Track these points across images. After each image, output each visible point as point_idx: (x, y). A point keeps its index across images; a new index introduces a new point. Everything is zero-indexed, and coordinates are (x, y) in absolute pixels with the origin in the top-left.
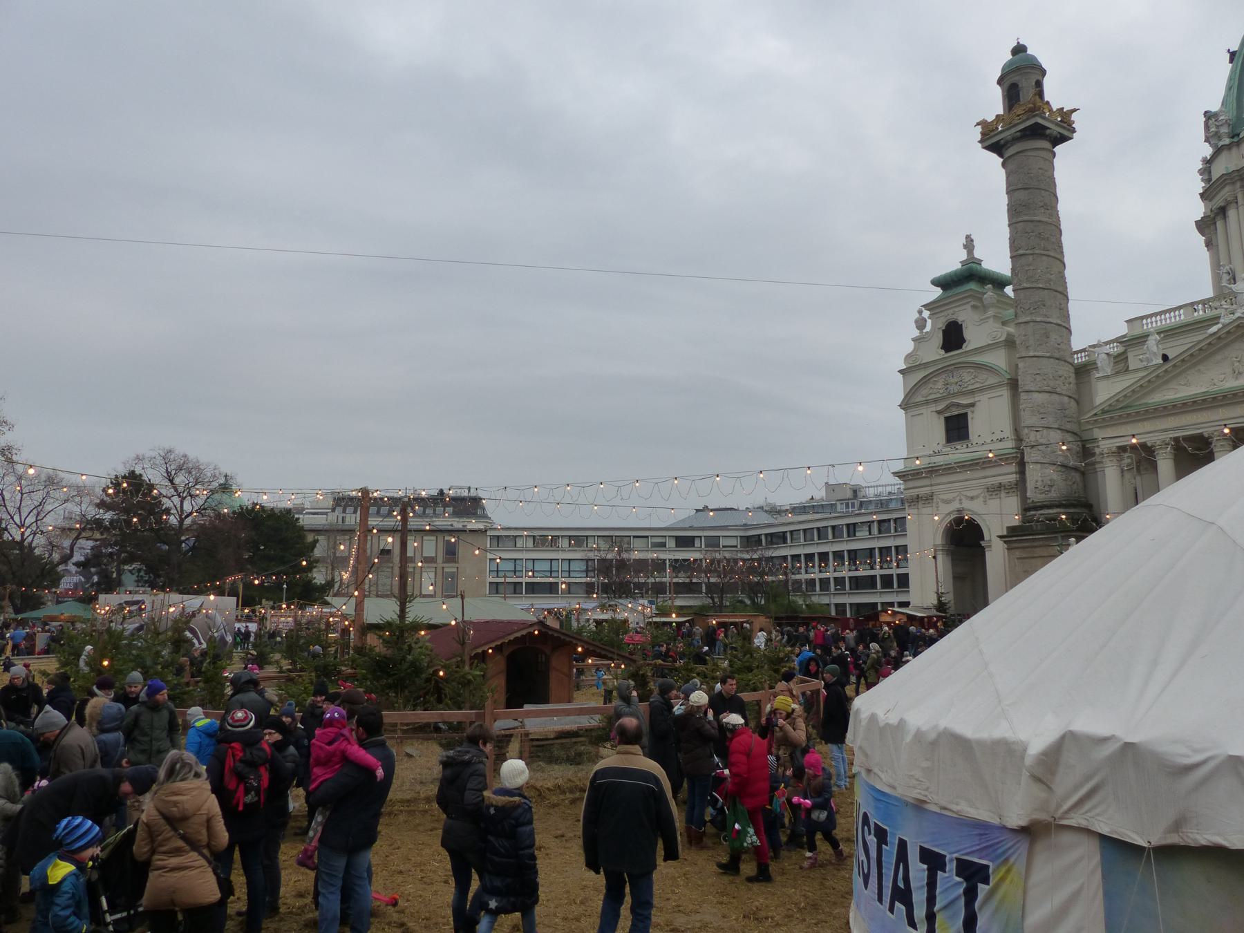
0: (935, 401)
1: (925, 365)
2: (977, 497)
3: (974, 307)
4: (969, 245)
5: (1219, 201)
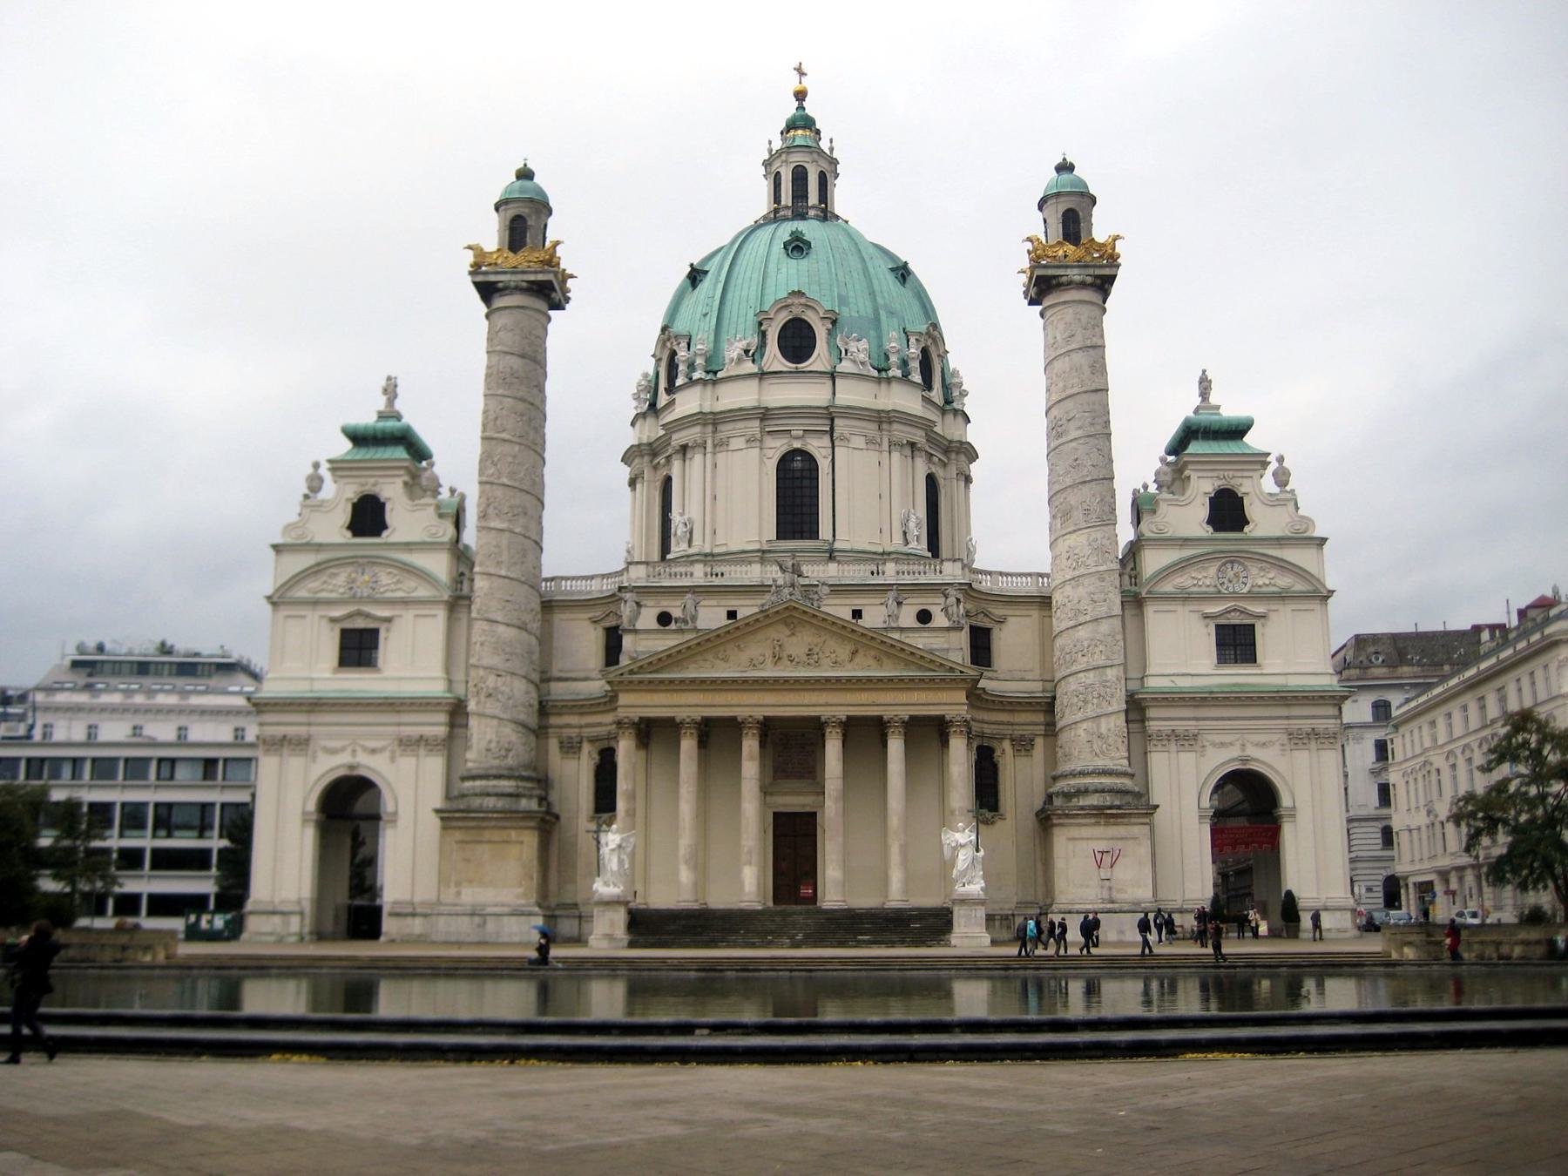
1: (320, 547)
3: (406, 484)
4: (391, 390)
5: (679, 439)
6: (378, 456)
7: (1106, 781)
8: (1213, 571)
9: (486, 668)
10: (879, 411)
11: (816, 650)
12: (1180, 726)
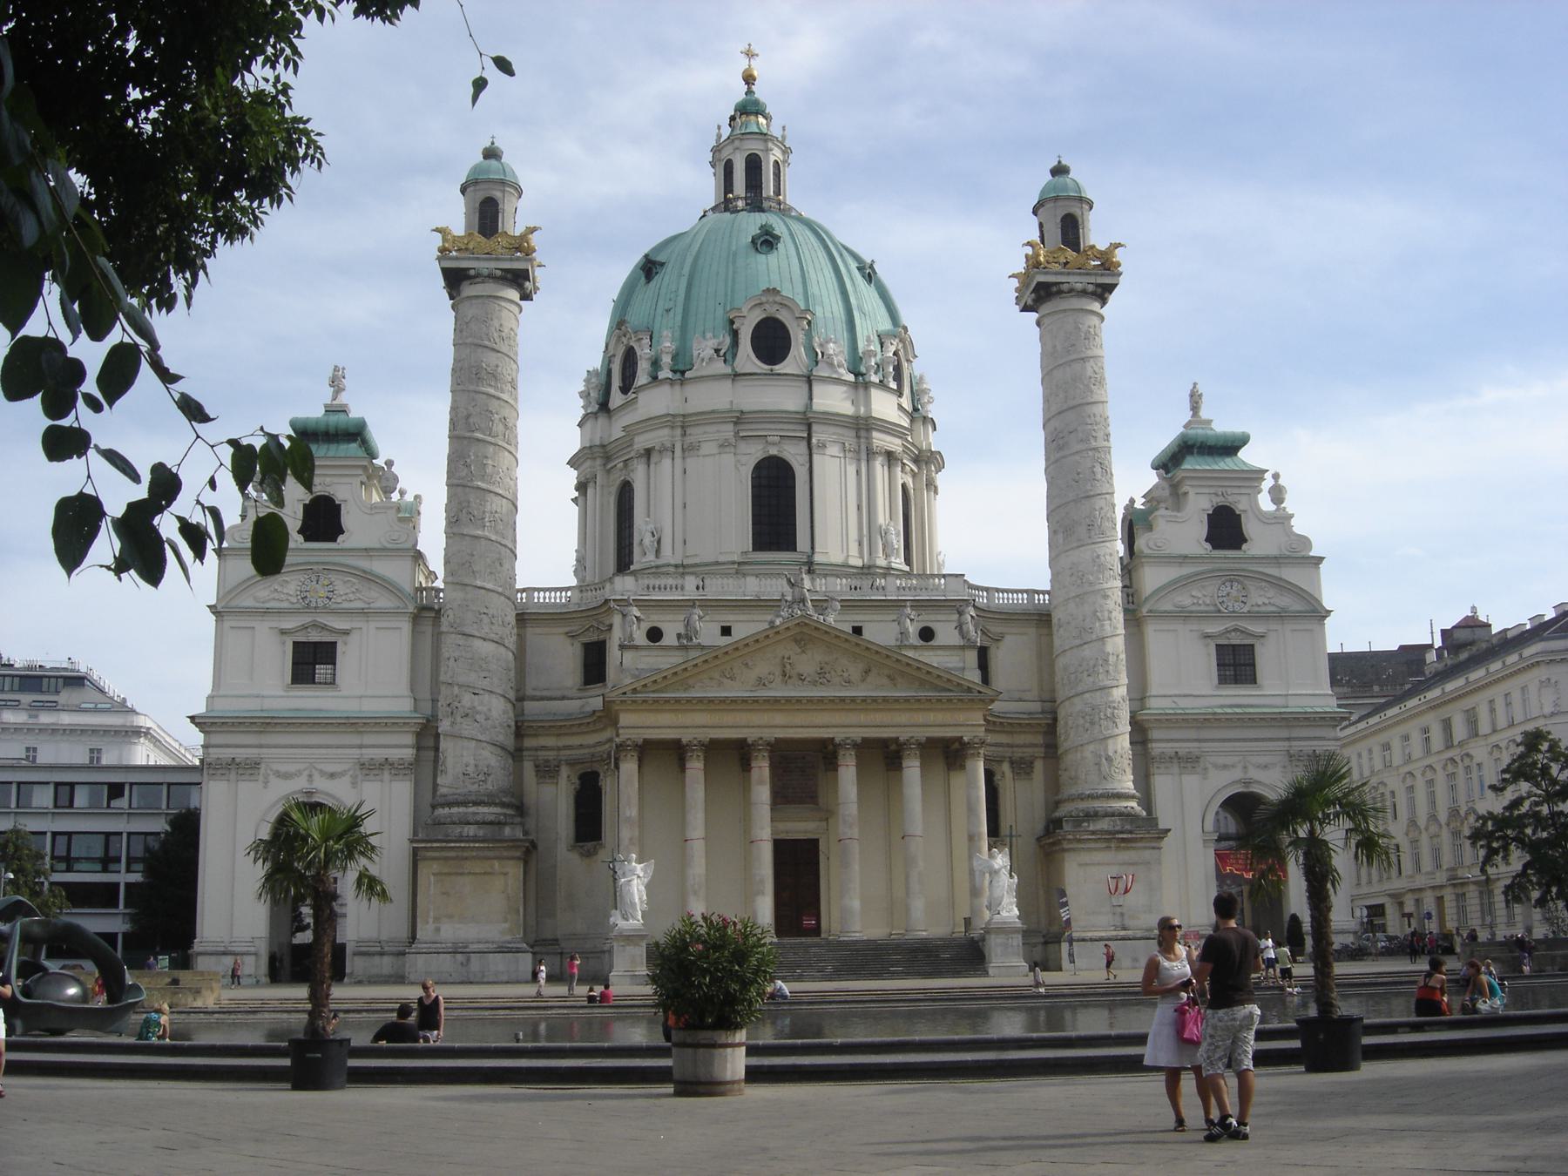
0: (280, 612)
2: (342, 774)
5: (642, 442)
6: (331, 454)
9: (460, 686)
10: (857, 418)
11: (827, 668)
12: (1183, 748)
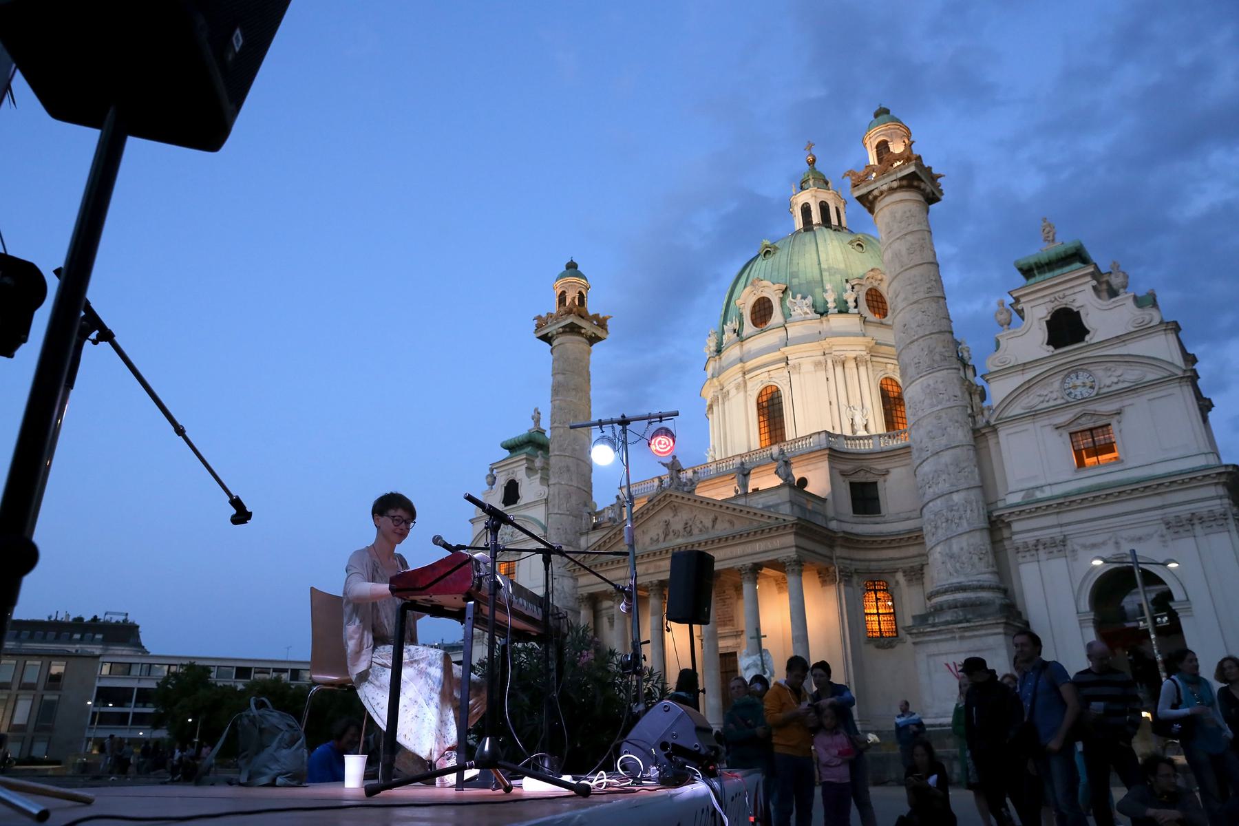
7: (960, 596)
8: (1057, 385)
12: (1044, 535)
